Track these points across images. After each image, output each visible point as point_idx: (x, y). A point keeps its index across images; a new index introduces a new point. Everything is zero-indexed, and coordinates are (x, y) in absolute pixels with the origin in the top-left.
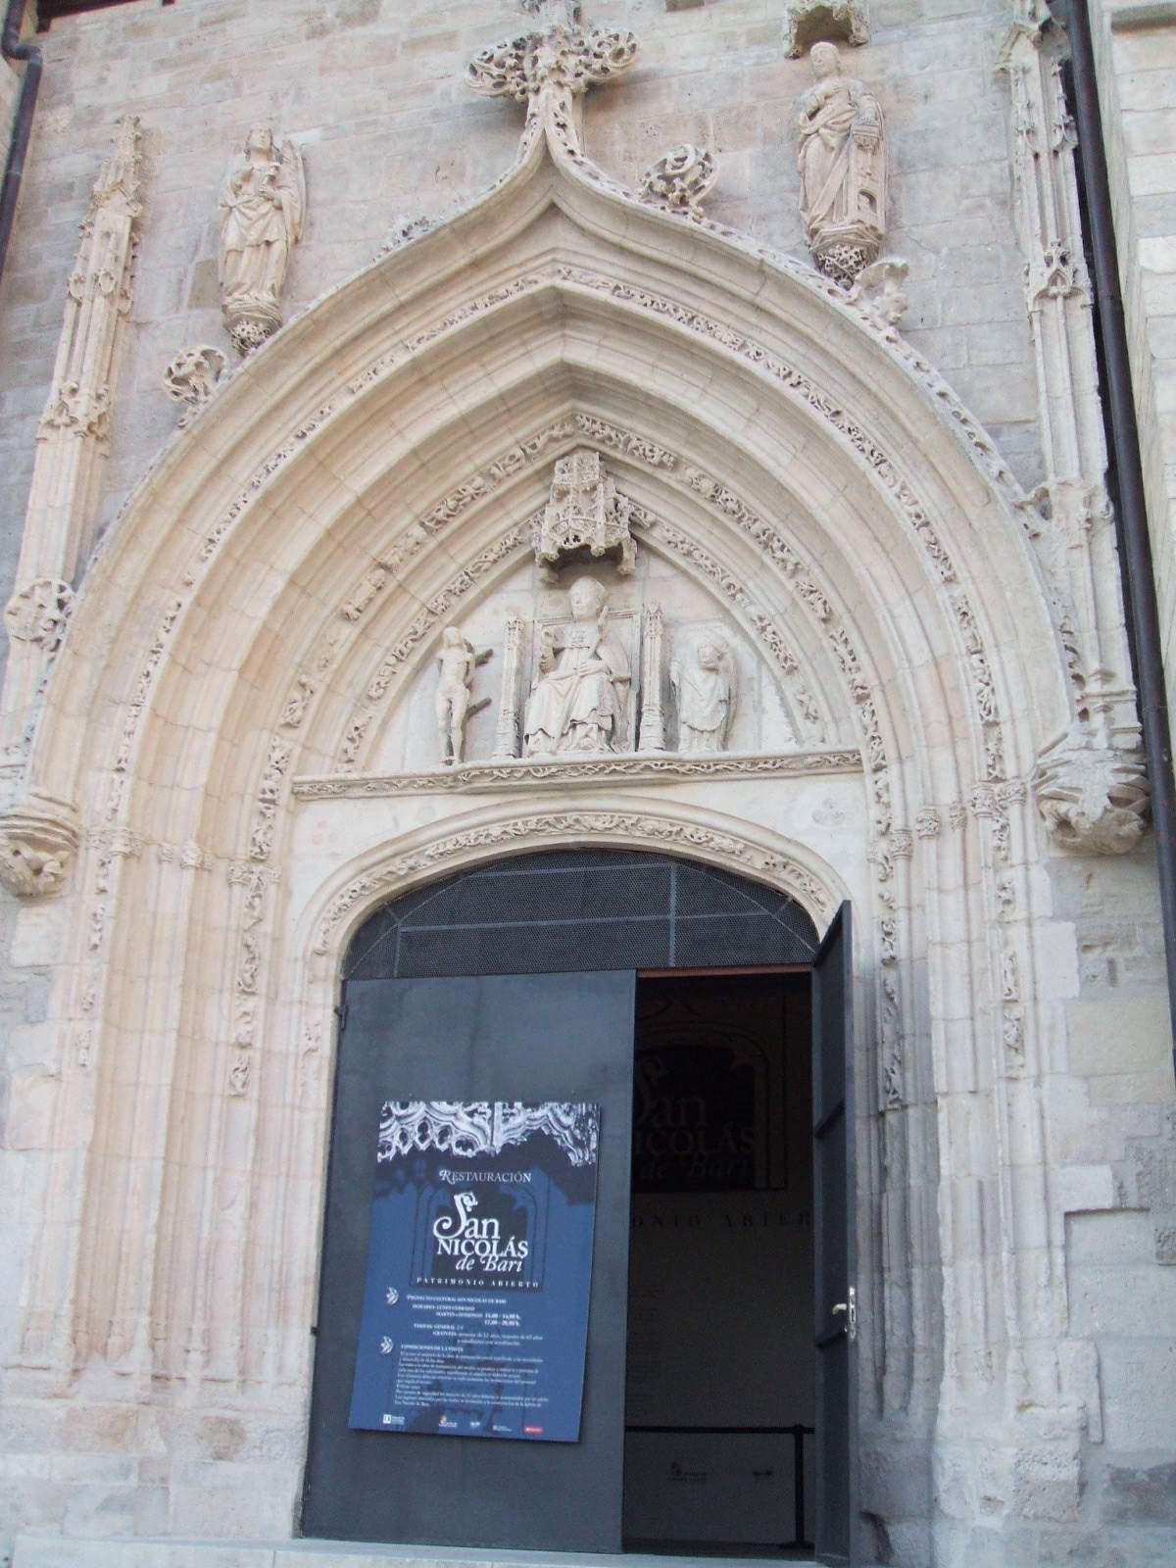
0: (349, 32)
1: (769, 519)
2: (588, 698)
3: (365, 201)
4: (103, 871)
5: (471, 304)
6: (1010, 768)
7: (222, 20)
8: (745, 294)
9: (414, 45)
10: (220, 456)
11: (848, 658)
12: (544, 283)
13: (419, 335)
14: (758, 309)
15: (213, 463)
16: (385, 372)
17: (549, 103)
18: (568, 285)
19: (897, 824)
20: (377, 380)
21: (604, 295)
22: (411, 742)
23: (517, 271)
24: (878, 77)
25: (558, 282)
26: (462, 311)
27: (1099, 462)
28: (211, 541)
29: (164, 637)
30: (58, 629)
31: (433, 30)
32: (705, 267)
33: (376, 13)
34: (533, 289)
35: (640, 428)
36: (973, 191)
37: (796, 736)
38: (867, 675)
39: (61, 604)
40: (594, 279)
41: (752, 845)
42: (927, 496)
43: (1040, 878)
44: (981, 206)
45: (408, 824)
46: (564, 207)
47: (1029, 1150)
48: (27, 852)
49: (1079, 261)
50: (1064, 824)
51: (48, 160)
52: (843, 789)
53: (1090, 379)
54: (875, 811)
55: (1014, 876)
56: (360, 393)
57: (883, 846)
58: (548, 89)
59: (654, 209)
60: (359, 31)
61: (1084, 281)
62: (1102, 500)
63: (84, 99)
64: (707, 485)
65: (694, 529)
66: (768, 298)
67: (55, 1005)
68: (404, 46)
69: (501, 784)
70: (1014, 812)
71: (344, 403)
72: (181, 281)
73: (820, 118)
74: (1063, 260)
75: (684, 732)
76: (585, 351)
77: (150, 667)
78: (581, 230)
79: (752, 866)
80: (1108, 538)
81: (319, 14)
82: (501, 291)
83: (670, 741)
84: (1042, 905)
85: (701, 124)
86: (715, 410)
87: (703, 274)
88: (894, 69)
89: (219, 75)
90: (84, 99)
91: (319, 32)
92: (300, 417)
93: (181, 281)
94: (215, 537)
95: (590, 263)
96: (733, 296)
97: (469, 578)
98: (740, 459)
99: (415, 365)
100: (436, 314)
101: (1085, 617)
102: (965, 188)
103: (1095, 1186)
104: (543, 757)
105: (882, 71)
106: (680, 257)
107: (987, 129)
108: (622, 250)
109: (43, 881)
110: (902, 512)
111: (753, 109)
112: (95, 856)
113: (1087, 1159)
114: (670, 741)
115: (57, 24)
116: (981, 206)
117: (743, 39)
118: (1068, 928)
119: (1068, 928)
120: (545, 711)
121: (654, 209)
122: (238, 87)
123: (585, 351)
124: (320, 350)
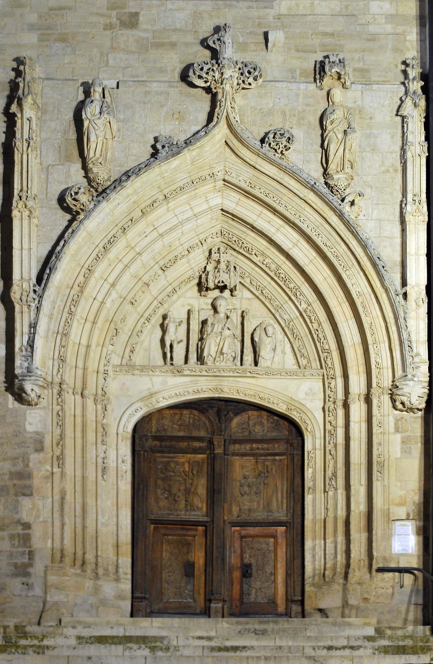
11: (322, 339)
33: (137, 24)
41: (284, 402)
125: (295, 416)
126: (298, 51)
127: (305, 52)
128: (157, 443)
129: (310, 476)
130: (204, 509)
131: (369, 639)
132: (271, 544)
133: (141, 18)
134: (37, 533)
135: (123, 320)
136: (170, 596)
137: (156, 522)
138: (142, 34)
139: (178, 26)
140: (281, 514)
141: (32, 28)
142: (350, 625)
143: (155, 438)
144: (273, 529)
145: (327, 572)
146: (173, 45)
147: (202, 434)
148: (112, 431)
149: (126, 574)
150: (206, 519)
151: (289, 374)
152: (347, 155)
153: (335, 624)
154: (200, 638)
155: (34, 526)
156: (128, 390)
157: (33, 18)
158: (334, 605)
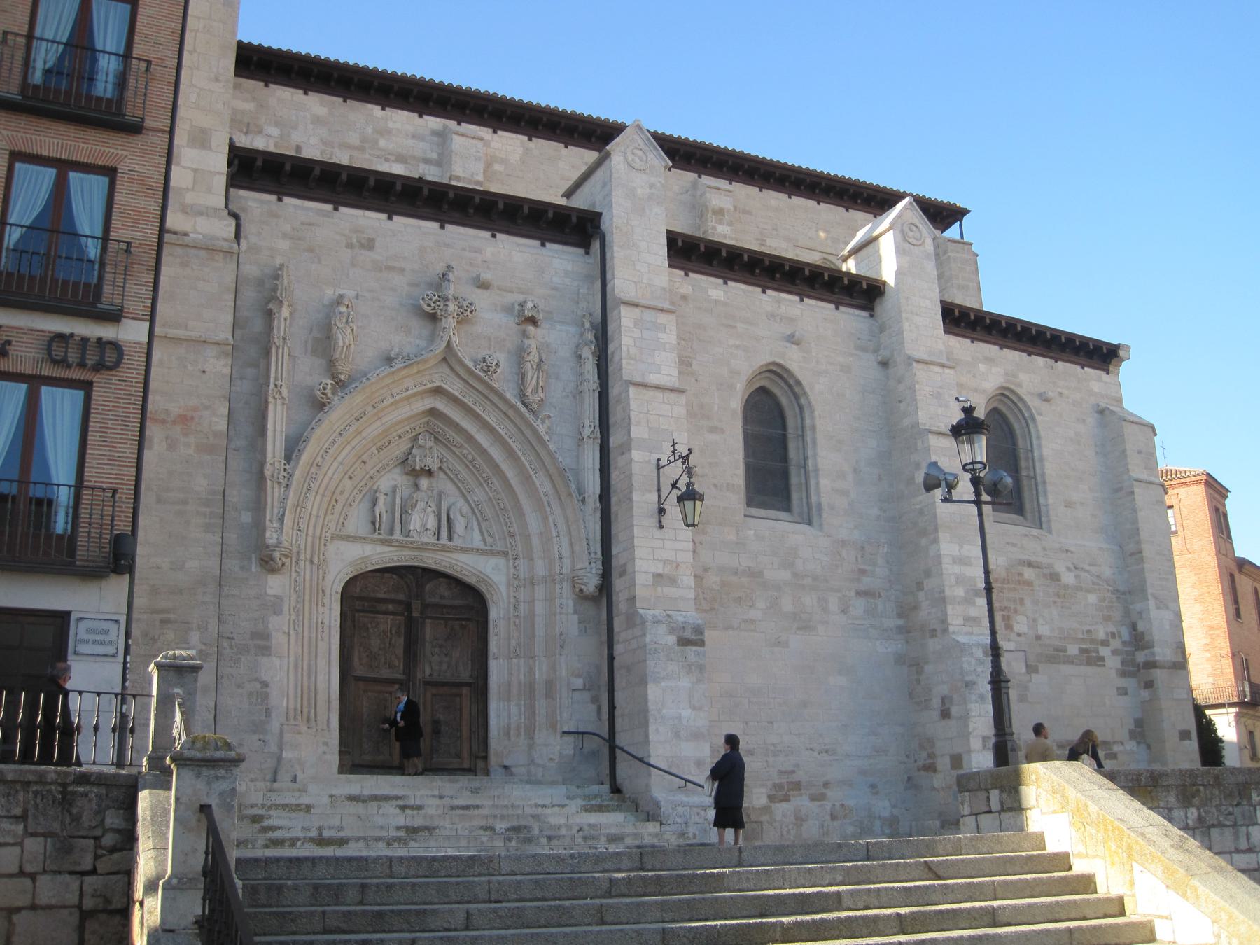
1: (488, 472)
2: (432, 522)
6: (564, 571)
7: (310, 224)
9: (391, 269)
12: (437, 384)
14: (505, 414)
17: (450, 323)
19: (522, 576)
21: (457, 394)
22: (357, 522)
27: (598, 491)
32: (492, 396)
35: (451, 434)
37: (484, 540)
38: (515, 529)
40: (455, 387)
41: (474, 574)
42: (548, 487)
43: (571, 603)
45: (367, 554)
47: (564, 673)
49: (598, 429)
50: (581, 591)
52: (501, 561)
53: (598, 466)
54: (512, 571)
55: (564, 601)
57: (517, 583)
58: (450, 319)
59: (482, 375)
62: (598, 504)
63: (253, 239)
64: (470, 457)
65: (460, 468)
66: (511, 413)
69: (401, 545)
70: (565, 583)
73: (531, 357)
75: (455, 536)
76: (441, 405)
78: (452, 369)
79: (472, 580)
80: (598, 515)
83: (450, 538)
84: (571, 610)
86: (482, 438)
89: (311, 250)
91: (350, 246)
96: (497, 407)
97: (384, 467)
98: (483, 452)
101: (591, 536)
103: (578, 683)
104: (416, 538)
106: (486, 392)
108: (464, 380)
110: (541, 490)
113: (579, 676)
114: (450, 538)
118: (576, 617)
119: (576, 617)
120: (415, 522)
121: (482, 375)
123: (441, 405)
133: (377, 244)
135: (342, 492)
140: (465, 674)
148: (328, 592)
150: (402, 677)
151: (479, 551)
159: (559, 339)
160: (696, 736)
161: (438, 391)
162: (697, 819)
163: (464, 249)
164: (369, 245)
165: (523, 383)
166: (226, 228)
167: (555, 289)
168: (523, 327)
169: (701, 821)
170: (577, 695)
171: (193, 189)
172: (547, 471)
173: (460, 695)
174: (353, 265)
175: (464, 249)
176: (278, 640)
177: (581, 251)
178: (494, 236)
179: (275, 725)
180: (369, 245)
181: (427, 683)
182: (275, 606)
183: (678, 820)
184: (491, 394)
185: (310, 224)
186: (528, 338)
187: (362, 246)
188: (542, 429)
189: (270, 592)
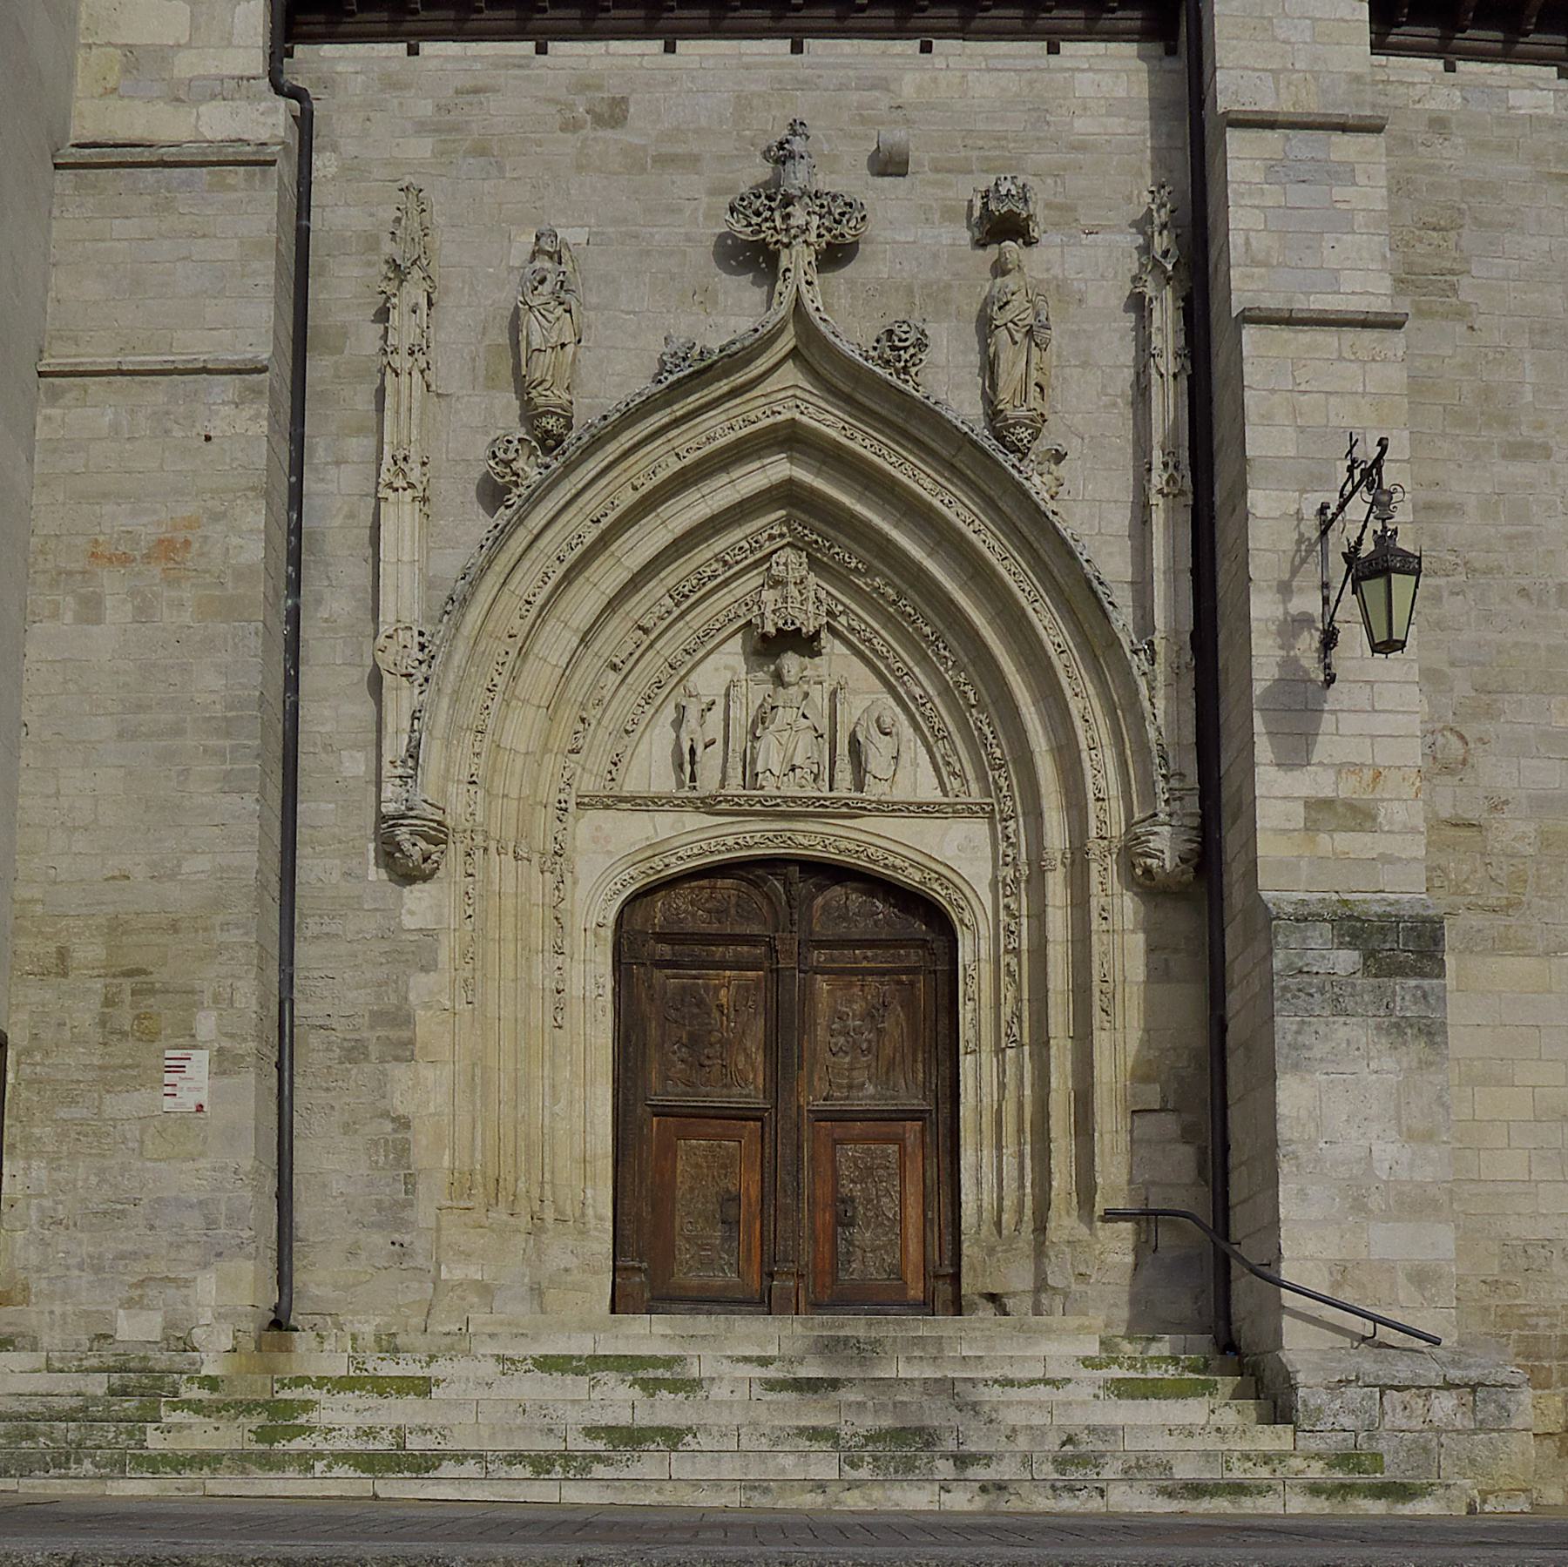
0: (600, 133)
3: (634, 313)
4: (469, 860)
5: (728, 424)
7: (476, 91)
8: (944, 453)
9: (666, 161)
10: (535, 532)
12: (786, 415)
13: (687, 445)
15: (530, 537)
16: (663, 475)
18: (804, 419)
20: (656, 480)
23: (763, 400)
24: (1045, 276)
25: (798, 416)
26: (719, 428)
28: (529, 603)
29: (497, 679)
30: (424, 667)
31: (681, 149)
34: (779, 418)
36: (1110, 391)
39: (422, 647)
40: (829, 422)
44: (1115, 405)
46: (805, 352)
48: (423, 844)
51: (323, 207)
56: (643, 490)
60: (609, 134)
61: (1188, 484)
62: (1187, 655)
67: (444, 956)
68: (654, 161)
71: (628, 498)
72: (473, 360)
74: (1176, 467)
77: (489, 703)
81: (571, 107)
82: (753, 418)
85: (910, 292)
87: (915, 432)
88: (1056, 271)
89: (481, 151)
90: (350, 148)
91: (571, 126)
92: (593, 504)
93: (473, 360)
94: (531, 599)
95: (823, 405)
99: (683, 471)
100: (700, 429)
102: (1104, 386)
105: (1048, 270)
107: (1122, 338)
109: (427, 866)
111: (949, 286)
112: (461, 848)
115: (299, 50)
116: (1115, 405)
117: (937, 216)
122: (501, 169)
124: (612, 450)
125: (939, 893)
126: (936, 170)
127: (949, 171)
128: (666, 948)
129: (969, 1016)
130: (760, 1080)
131: (1088, 1362)
132: (894, 1158)
134: (421, 1139)
136: (688, 1275)
137: (662, 1112)
138: (637, 141)
139: (704, 122)
141: (422, 128)
142: (1048, 1331)
143: (661, 937)
144: (896, 1127)
145: (1005, 1217)
146: (695, 159)
147: (755, 929)
149: (601, 1219)
152: (1034, 374)
153: (1021, 1328)
154: (747, 1360)
155: (415, 1123)
156: (607, 840)
157: (425, 108)
158: (1020, 1287)
159: (1092, 264)
160: (1416, 1205)
161: (790, 438)
162: (1401, 1422)
163: (841, 87)
164: (614, 114)
165: (994, 386)
166: (270, 121)
167: (1081, 147)
168: (992, 251)
169: (1417, 1424)
170: (1147, 1125)
171: (189, 46)
172: (1061, 592)
173: (899, 1141)
174: (580, 168)
175: (841, 87)
176: (426, 1025)
177: (1156, 48)
178: (926, 48)
179: (423, 1213)
180: (614, 114)
181: (821, 1116)
182: (419, 953)
183: (1347, 1421)
184: (916, 423)
185: (476, 91)
186: (1005, 273)
187: (599, 120)
188: (1037, 485)
189: (409, 922)
